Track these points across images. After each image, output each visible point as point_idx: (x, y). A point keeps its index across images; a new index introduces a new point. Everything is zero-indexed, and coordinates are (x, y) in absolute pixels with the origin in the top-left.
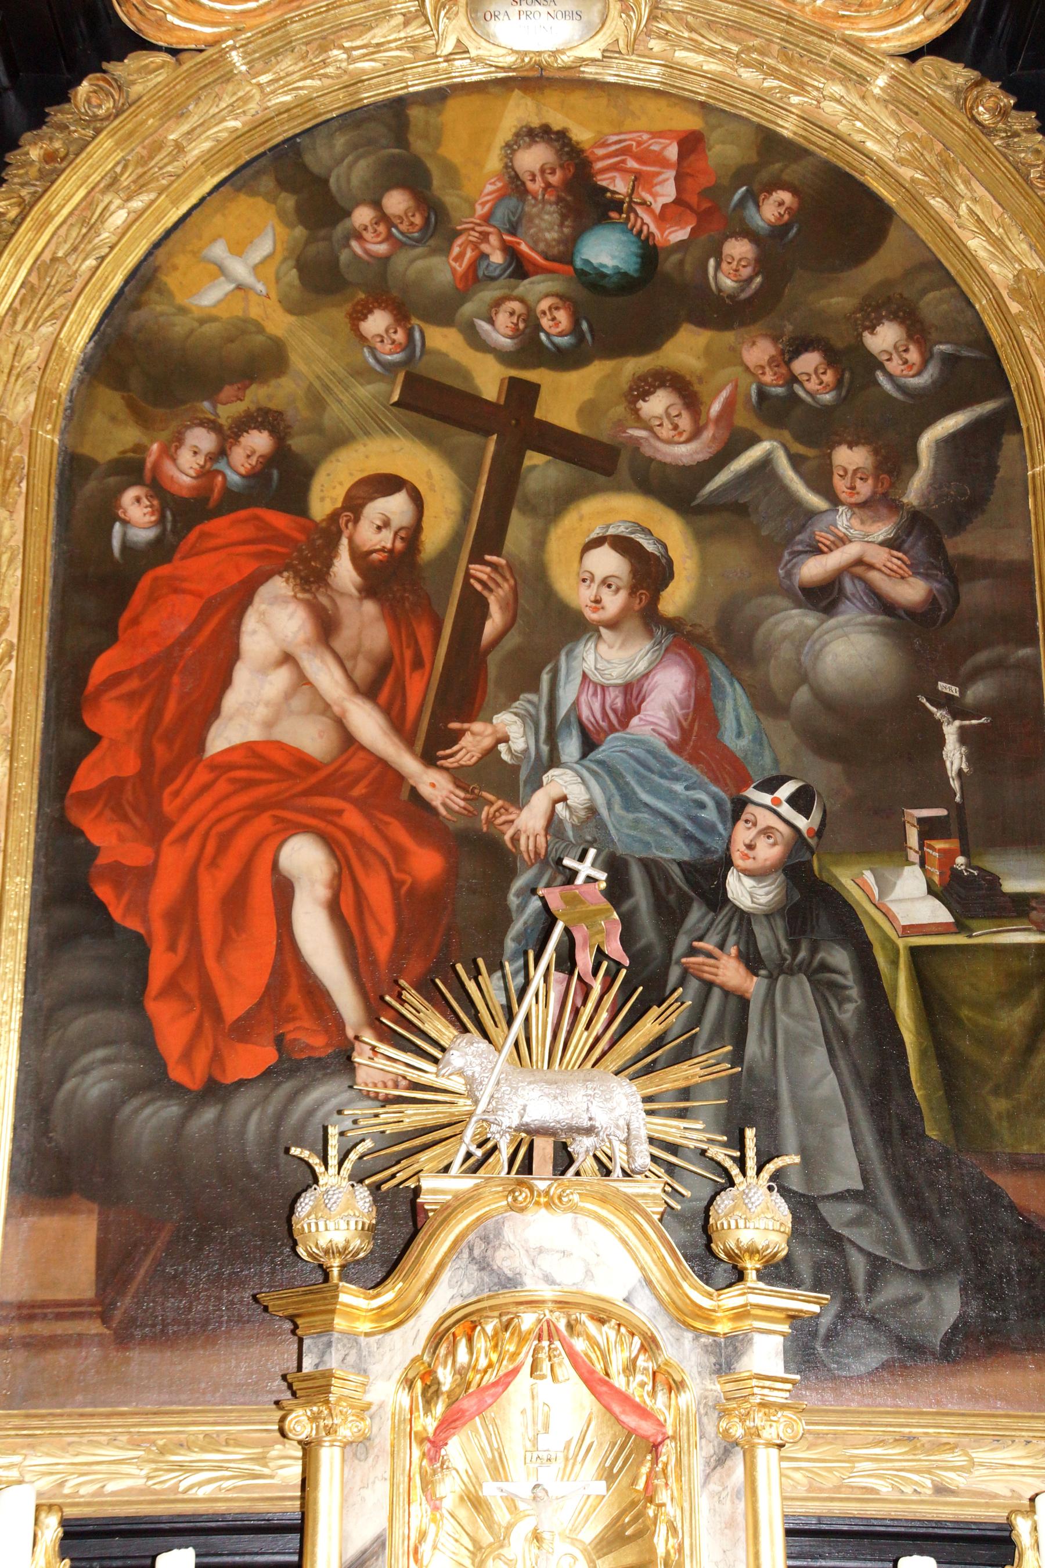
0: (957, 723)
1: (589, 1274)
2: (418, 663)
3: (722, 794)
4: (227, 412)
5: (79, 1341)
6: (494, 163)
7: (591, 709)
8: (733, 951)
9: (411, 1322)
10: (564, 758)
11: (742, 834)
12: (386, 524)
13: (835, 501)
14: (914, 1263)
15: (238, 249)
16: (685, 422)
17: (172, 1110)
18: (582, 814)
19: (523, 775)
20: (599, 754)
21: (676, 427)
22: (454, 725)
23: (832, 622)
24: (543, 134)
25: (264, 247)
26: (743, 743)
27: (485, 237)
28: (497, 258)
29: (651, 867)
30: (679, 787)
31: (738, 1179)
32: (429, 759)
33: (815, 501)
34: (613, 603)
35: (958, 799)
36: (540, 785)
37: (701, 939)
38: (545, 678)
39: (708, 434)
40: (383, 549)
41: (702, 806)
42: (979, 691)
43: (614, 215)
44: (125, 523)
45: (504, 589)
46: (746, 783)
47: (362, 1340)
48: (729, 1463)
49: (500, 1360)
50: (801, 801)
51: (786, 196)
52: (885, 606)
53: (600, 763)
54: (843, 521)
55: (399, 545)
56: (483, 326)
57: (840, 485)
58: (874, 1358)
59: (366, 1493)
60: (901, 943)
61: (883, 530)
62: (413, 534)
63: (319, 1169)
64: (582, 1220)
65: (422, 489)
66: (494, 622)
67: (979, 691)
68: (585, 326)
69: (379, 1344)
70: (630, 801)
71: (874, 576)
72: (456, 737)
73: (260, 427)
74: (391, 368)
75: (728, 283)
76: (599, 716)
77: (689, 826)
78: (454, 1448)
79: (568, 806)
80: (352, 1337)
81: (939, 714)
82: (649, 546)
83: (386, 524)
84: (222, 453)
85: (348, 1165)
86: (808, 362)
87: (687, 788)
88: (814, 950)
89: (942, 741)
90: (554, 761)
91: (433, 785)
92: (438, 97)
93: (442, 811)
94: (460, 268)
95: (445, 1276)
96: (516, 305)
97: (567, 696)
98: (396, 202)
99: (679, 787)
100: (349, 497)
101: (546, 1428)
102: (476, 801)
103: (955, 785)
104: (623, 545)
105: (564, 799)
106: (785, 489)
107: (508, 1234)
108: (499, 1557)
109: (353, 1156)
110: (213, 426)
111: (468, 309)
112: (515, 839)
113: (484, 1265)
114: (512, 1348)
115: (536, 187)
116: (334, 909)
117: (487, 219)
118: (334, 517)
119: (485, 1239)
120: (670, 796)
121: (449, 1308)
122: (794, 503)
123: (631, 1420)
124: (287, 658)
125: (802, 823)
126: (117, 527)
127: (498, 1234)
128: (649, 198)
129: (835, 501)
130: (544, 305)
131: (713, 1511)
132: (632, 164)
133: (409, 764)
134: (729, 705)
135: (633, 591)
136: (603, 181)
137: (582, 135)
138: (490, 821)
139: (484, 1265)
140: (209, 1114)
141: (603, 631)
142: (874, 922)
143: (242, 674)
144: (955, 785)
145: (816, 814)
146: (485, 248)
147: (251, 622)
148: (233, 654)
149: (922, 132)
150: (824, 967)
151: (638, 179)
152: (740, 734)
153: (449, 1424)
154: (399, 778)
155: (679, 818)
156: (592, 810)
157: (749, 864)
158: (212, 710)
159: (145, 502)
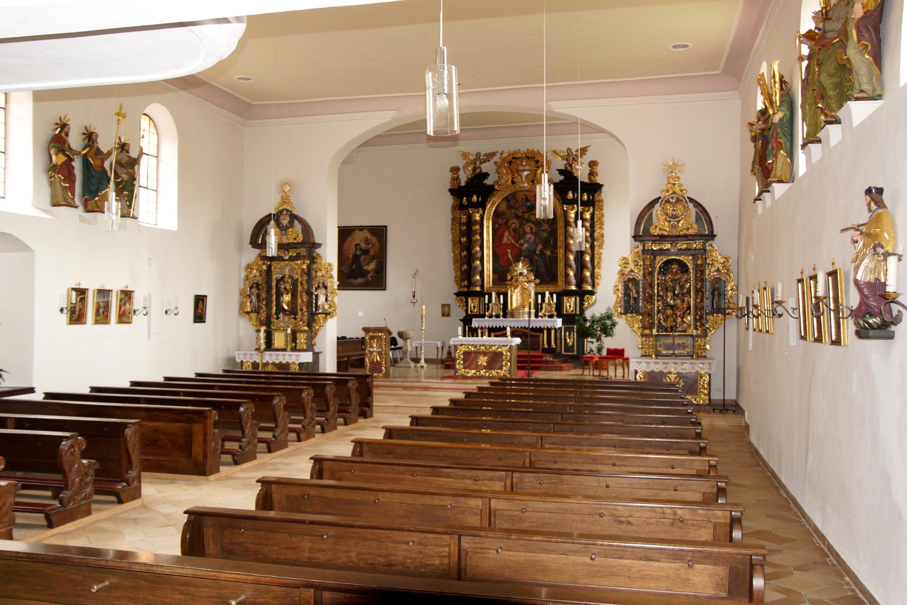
24: (524, 195)
34: (529, 231)
52: (547, 231)
54: (545, 225)
92: (516, 192)
98: (514, 201)
133: (515, 244)
158: (502, 240)
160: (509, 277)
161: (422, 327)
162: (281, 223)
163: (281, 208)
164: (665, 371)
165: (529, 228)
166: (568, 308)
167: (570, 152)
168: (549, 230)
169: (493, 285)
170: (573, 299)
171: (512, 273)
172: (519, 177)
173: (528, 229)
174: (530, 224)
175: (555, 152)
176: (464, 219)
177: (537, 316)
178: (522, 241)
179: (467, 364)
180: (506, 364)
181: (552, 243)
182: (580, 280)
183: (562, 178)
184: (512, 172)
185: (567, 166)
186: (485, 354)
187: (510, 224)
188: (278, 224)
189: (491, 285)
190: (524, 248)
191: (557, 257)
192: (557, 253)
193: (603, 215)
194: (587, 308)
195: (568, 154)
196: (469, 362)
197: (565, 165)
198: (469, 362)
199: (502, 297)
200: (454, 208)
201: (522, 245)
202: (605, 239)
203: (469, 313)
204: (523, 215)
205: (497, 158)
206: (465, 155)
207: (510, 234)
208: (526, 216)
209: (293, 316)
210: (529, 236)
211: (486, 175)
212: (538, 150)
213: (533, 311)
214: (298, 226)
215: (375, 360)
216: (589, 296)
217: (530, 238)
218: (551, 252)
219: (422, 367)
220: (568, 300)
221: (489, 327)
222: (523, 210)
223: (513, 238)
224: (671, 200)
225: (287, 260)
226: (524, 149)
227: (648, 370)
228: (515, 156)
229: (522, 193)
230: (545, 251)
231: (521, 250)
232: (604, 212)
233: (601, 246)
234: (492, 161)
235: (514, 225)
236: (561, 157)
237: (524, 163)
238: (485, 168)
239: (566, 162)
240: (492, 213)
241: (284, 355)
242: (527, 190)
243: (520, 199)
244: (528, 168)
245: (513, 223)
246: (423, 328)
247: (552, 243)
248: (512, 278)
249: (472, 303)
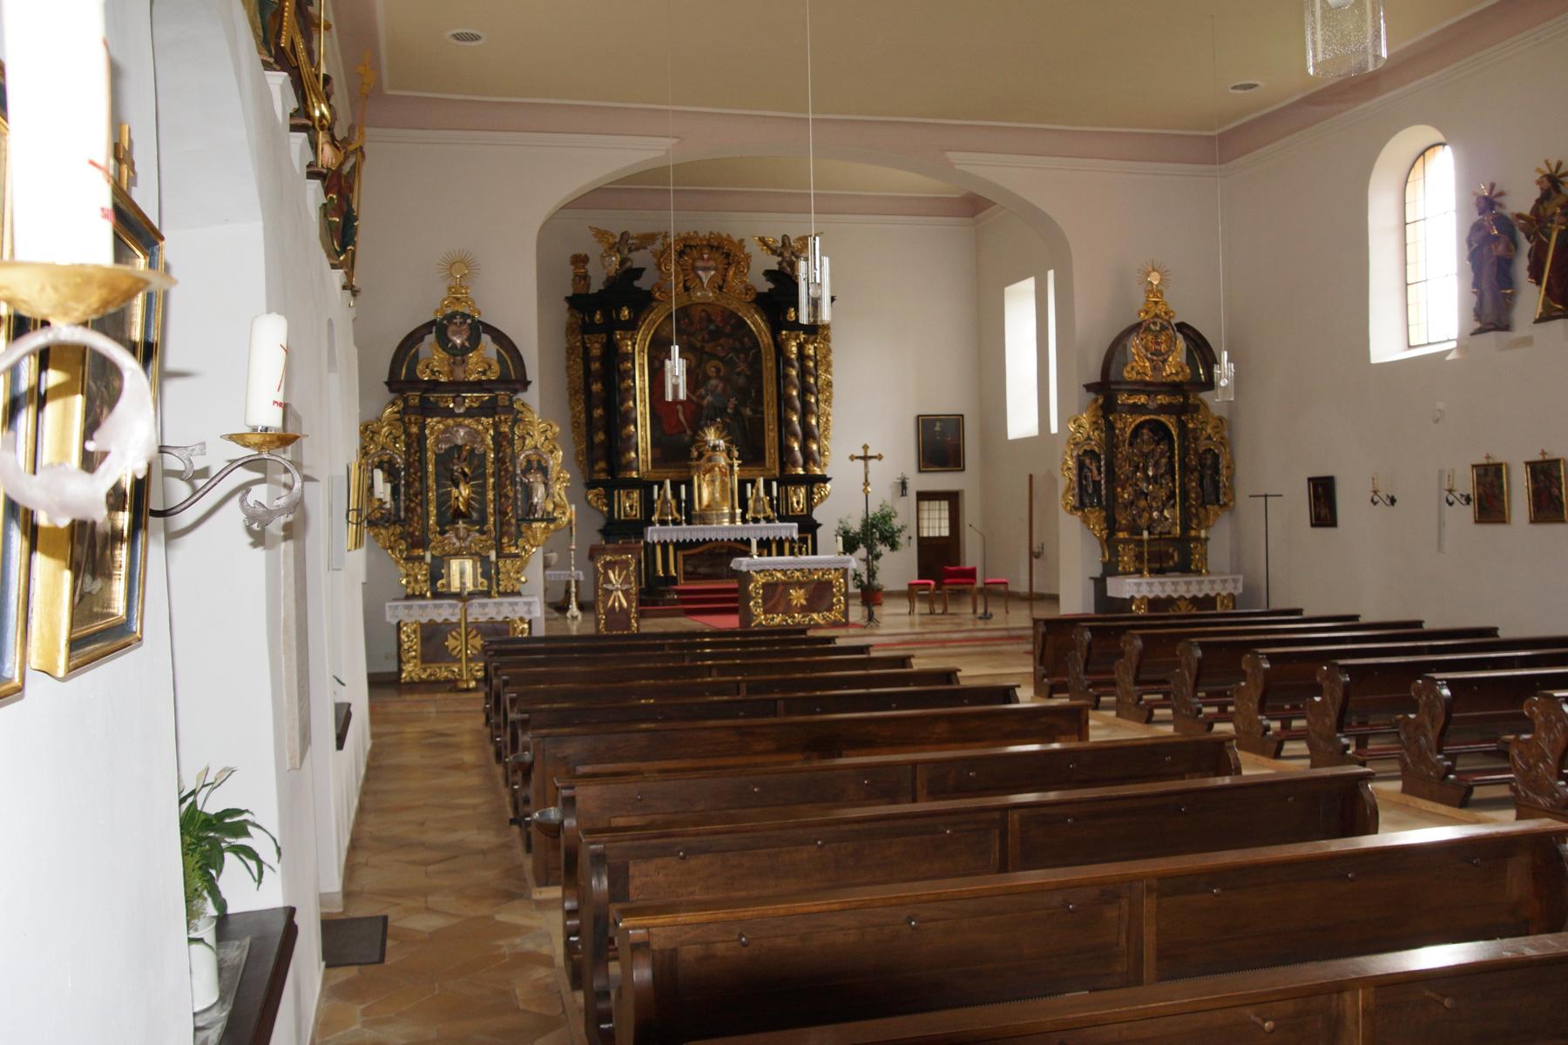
24: (703, 311)
33: (736, 360)
34: (714, 374)
54: (741, 364)
66: (700, 377)
78: (707, 476)
89: (751, 393)
92: (690, 305)
97: (709, 387)
98: (686, 320)
104: (716, 368)
137: (709, 311)
160: (695, 454)
161: (571, 545)
162: (450, 341)
163: (449, 311)
164: (1175, 596)
165: (713, 369)
166: (795, 505)
167: (787, 242)
168: (749, 373)
169: (653, 467)
170: (803, 490)
171: (700, 447)
172: (697, 280)
173: (712, 371)
174: (715, 362)
175: (762, 240)
176: (596, 350)
177: (744, 521)
178: (702, 391)
179: (770, 605)
180: (839, 600)
181: (753, 394)
182: (808, 457)
183: (771, 286)
184: (683, 270)
185: (785, 264)
186: (800, 585)
188: (443, 341)
189: (650, 467)
190: (705, 402)
191: (763, 419)
192: (762, 413)
193: (829, 351)
194: (816, 504)
195: (784, 245)
196: (773, 602)
197: (780, 264)
198: (773, 602)
199: (683, 487)
200: (570, 330)
201: (702, 397)
202: (835, 389)
203: (622, 518)
204: (703, 347)
205: (658, 246)
206: (601, 234)
208: (708, 347)
209: (477, 527)
210: (713, 382)
211: (638, 273)
212: (728, 236)
213: (739, 511)
214: (488, 346)
215: (617, 609)
216: (822, 485)
217: (717, 386)
218: (752, 410)
219: (574, 618)
220: (794, 491)
221: (678, 541)
224: (1152, 326)
225: (460, 415)
226: (704, 232)
227: (1151, 596)
228: (688, 242)
229: (701, 307)
230: (742, 409)
231: (700, 406)
232: (832, 345)
233: (828, 401)
234: (650, 248)
236: (771, 249)
237: (706, 256)
238: (639, 259)
239: (780, 259)
240: (647, 343)
241: (483, 606)
242: (709, 304)
244: (712, 263)
246: (573, 547)
247: (753, 394)
248: (701, 456)
249: (629, 503)
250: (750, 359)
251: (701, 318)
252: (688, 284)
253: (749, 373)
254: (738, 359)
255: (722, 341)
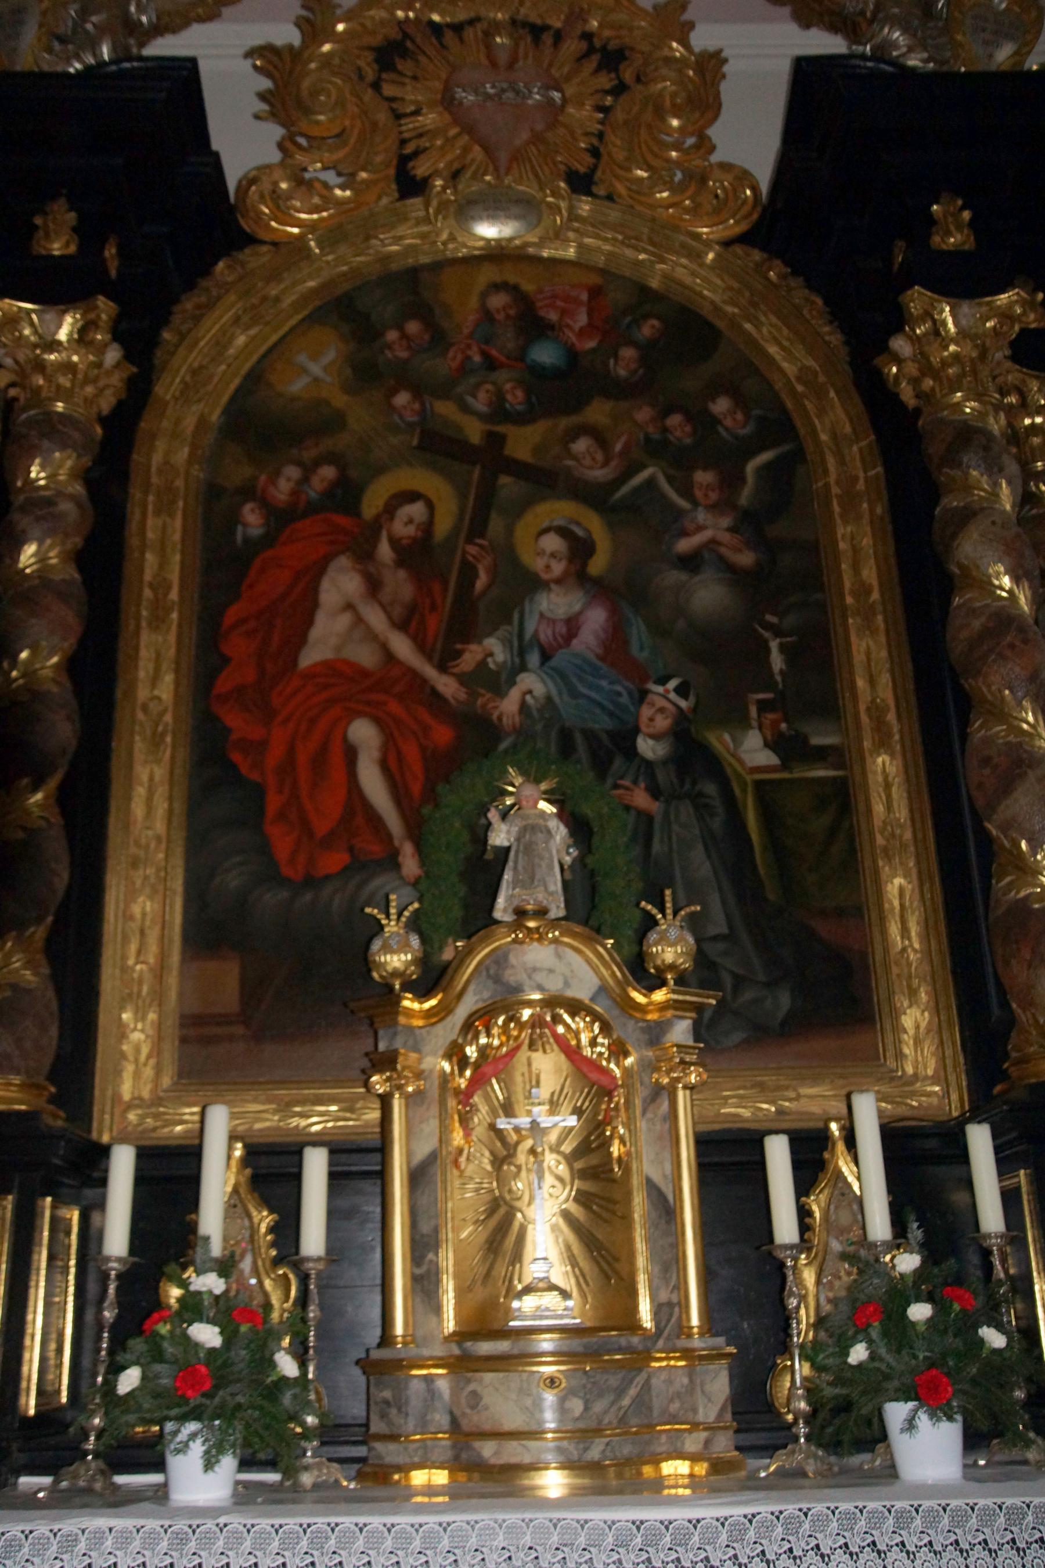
0: (778, 640)
1: (567, 984)
2: (433, 608)
3: (631, 686)
4: (309, 454)
5: (231, 1038)
6: (474, 302)
7: (546, 635)
8: (642, 785)
9: (449, 1019)
10: (530, 666)
11: (646, 712)
12: (411, 521)
13: (695, 503)
14: (761, 977)
15: (314, 357)
16: (600, 456)
17: (285, 894)
18: (542, 701)
19: (504, 677)
20: (554, 662)
21: (593, 459)
22: (459, 646)
23: (697, 579)
25: (331, 355)
26: (645, 654)
27: (469, 347)
28: (477, 358)
29: (589, 735)
30: (604, 683)
31: (662, 921)
32: (443, 667)
33: (683, 503)
34: (558, 568)
35: (780, 686)
36: (514, 683)
37: (621, 778)
38: (516, 616)
39: (614, 463)
40: (409, 537)
41: (619, 694)
42: (791, 620)
43: (549, 333)
44: (245, 525)
45: (488, 560)
46: (645, 678)
47: (417, 1032)
48: (658, 1101)
49: (508, 1040)
50: (682, 691)
51: (655, 322)
52: (730, 568)
53: (553, 669)
54: (702, 516)
55: (419, 534)
56: (470, 400)
57: (698, 494)
58: (737, 1037)
59: (423, 1126)
60: (749, 778)
61: (726, 522)
62: (428, 528)
63: (384, 922)
64: (561, 949)
65: (435, 500)
67: (791, 620)
68: (534, 399)
69: (428, 1033)
70: (574, 694)
71: (723, 550)
72: (459, 654)
73: (330, 463)
74: (411, 425)
75: (622, 373)
76: (551, 638)
77: (611, 707)
79: (533, 697)
80: (411, 1029)
81: (767, 634)
82: (580, 532)
83: (411, 521)
84: (305, 479)
85: (403, 919)
86: (675, 420)
87: (611, 683)
88: (694, 783)
89: (768, 651)
90: (523, 668)
91: (446, 685)
92: (439, 266)
93: (452, 701)
94: (454, 365)
95: (472, 988)
96: (489, 387)
97: (530, 628)
98: (413, 327)
99: (604, 683)
100: (387, 505)
101: (538, 1085)
102: (473, 695)
103: (779, 678)
104: (563, 532)
105: (530, 692)
106: (663, 496)
107: (513, 959)
108: (510, 1164)
109: (406, 913)
110: (299, 463)
111: (459, 389)
112: (500, 718)
113: (497, 980)
114: (515, 1033)
115: (500, 317)
116: (384, 765)
117: (471, 335)
118: (377, 518)
119: (497, 963)
120: (598, 689)
121: (474, 1008)
122: (671, 506)
123: (594, 1076)
124: (349, 606)
125: (683, 704)
126: (240, 528)
127: (506, 957)
128: (571, 323)
129: (695, 503)
130: (508, 386)
131: (649, 1130)
132: (559, 303)
133: (430, 672)
134: (634, 631)
135: (571, 560)
136: (542, 313)
137: (528, 287)
138: (484, 706)
139: (497, 980)
140: (308, 897)
141: (553, 586)
142: (730, 764)
143: (321, 619)
144: (779, 678)
145: (692, 699)
146: (469, 353)
147: (325, 584)
148: (315, 605)
149: (736, 285)
150: (701, 794)
151: (564, 312)
152: (642, 649)
153: (478, 1081)
154: (424, 681)
155: (605, 703)
156: (549, 699)
157: (651, 730)
159: (257, 511)
165: (552, 543)
168: (746, 559)
181: (777, 662)
187: (372, 503)
190: (509, 706)
204: (495, 441)
207: (373, 586)
217: (573, 625)
218: (773, 744)
222: (500, 397)
223: (402, 625)
229: (488, 274)
230: (720, 740)
235: (416, 510)
243: (467, 315)
245: (412, 497)
247: (777, 662)
250: (745, 496)
251: (487, 316)
252: (421, 169)
253: (746, 559)
254: (686, 491)
255: (598, 412)
